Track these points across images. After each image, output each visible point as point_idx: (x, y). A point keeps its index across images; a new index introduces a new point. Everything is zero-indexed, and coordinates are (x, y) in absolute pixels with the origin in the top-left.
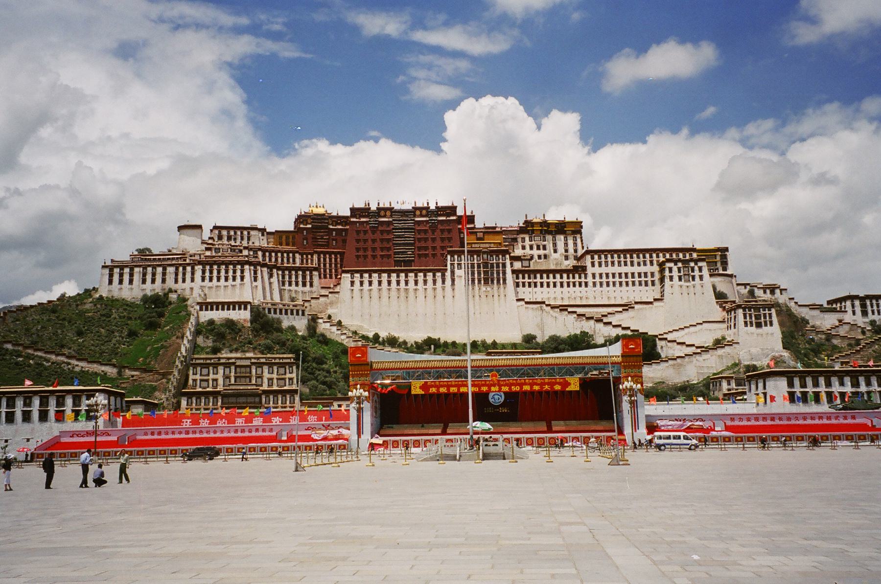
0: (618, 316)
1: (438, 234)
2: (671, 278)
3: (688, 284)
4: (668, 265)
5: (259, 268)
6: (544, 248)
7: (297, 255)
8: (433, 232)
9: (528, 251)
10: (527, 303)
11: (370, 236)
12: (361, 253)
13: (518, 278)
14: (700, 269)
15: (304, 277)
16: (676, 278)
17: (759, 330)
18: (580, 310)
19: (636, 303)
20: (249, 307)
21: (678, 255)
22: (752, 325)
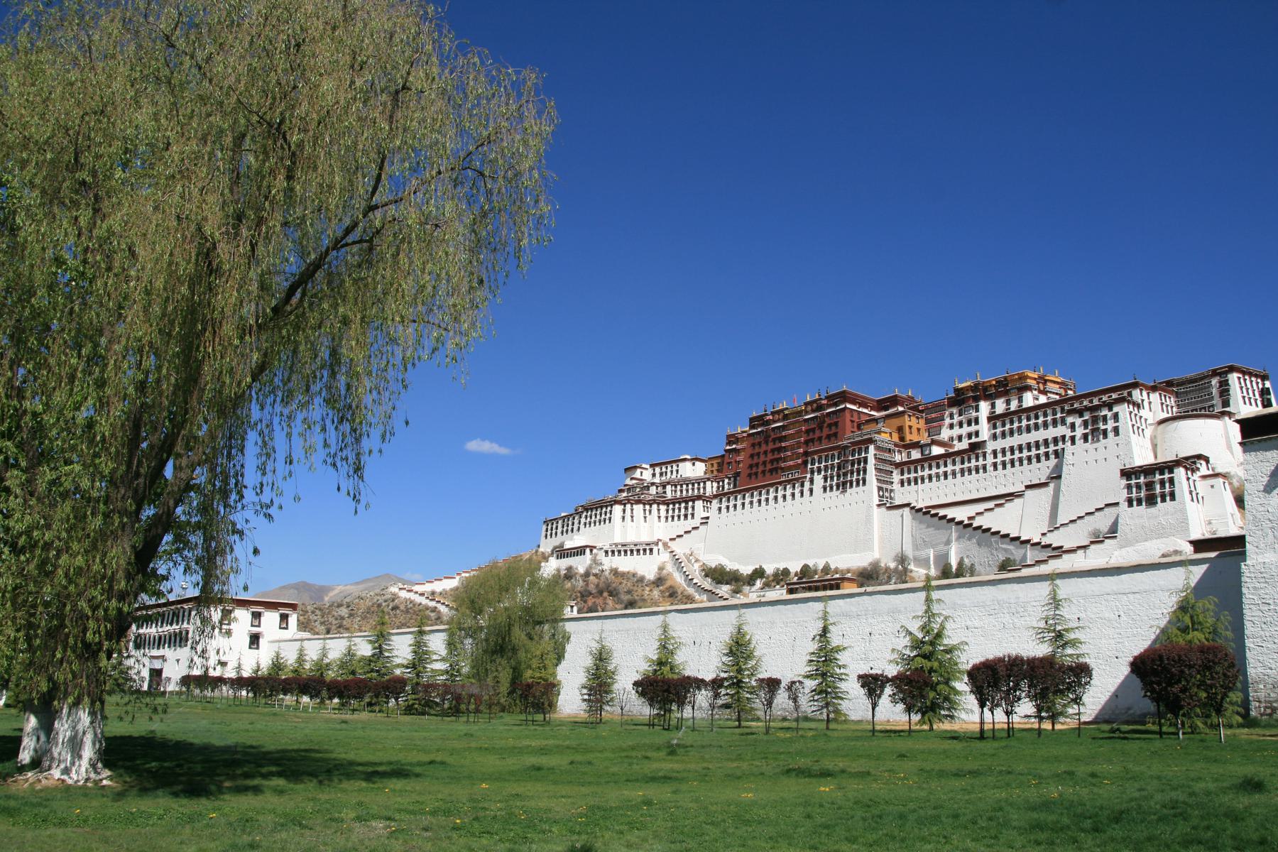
0: (997, 510)
1: (826, 431)
2: (1073, 442)
3: (1096, 445)
4: (1070, 420)
5: (628, 506)
6: (977, 422)
7: (709, 484)
8: (821, 428)
9: (957, 431)
10: (889, 508)
11: (764, 447)
12: (754, 470)
13: (902, 474)
14: (1116, 417)
15: (686, 508)
16: (1079, 442)
17: (1152, 510)
18: (942, 512)
19: (1028, 487)
20: (588, 551)
21: (1091, 402)
22: (1139, 502)
